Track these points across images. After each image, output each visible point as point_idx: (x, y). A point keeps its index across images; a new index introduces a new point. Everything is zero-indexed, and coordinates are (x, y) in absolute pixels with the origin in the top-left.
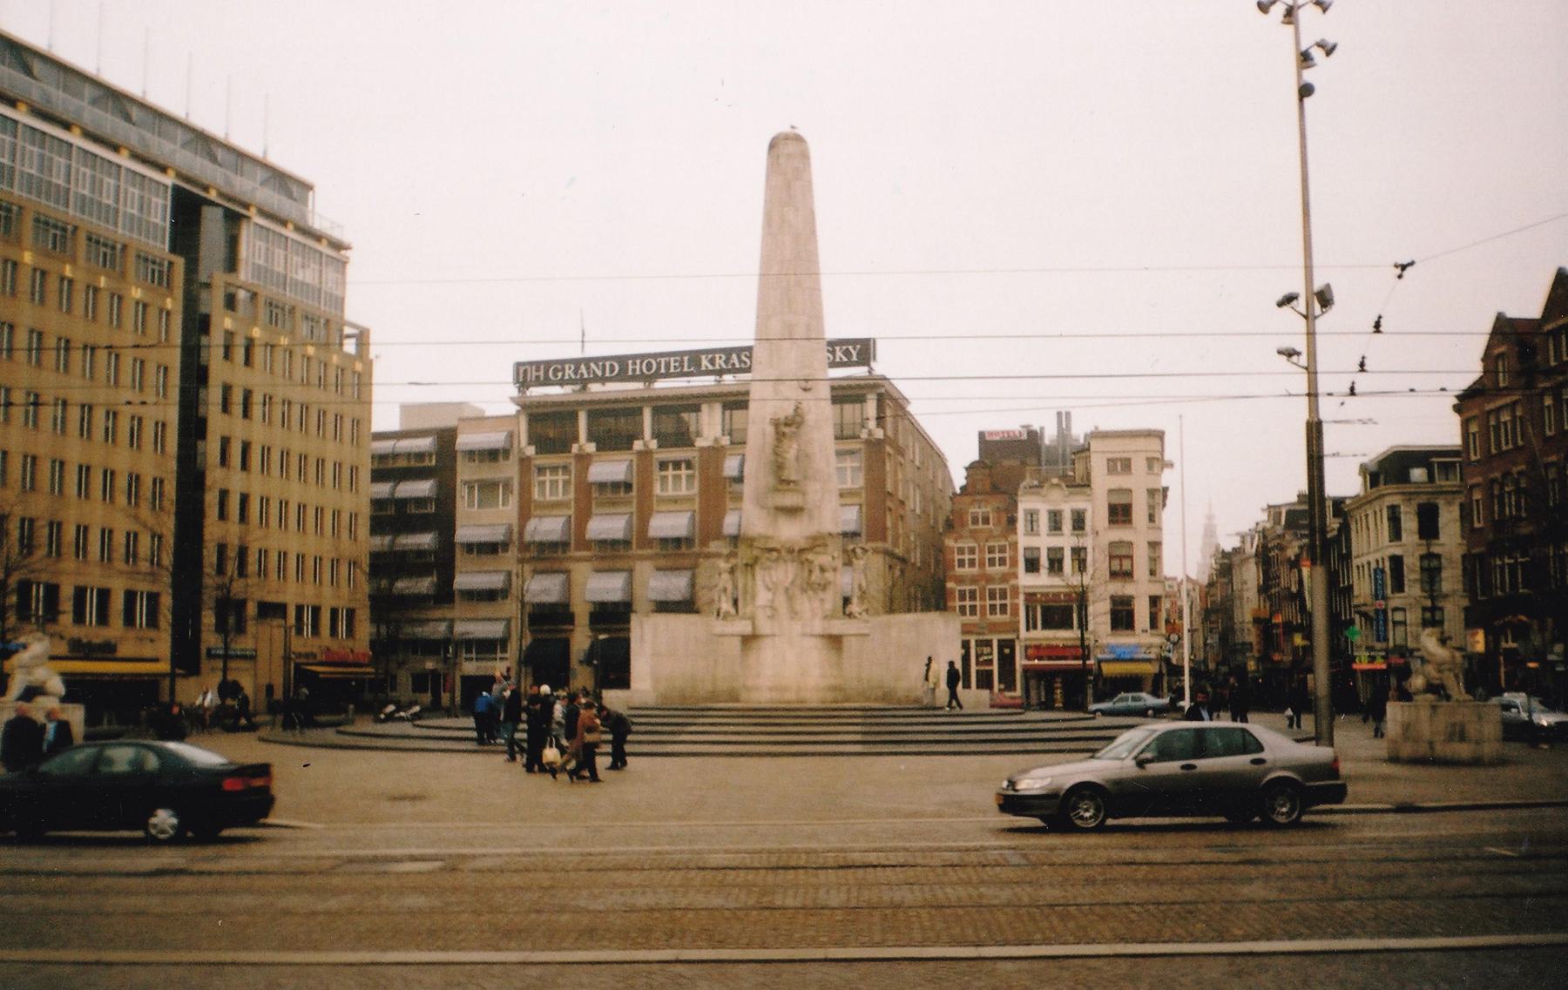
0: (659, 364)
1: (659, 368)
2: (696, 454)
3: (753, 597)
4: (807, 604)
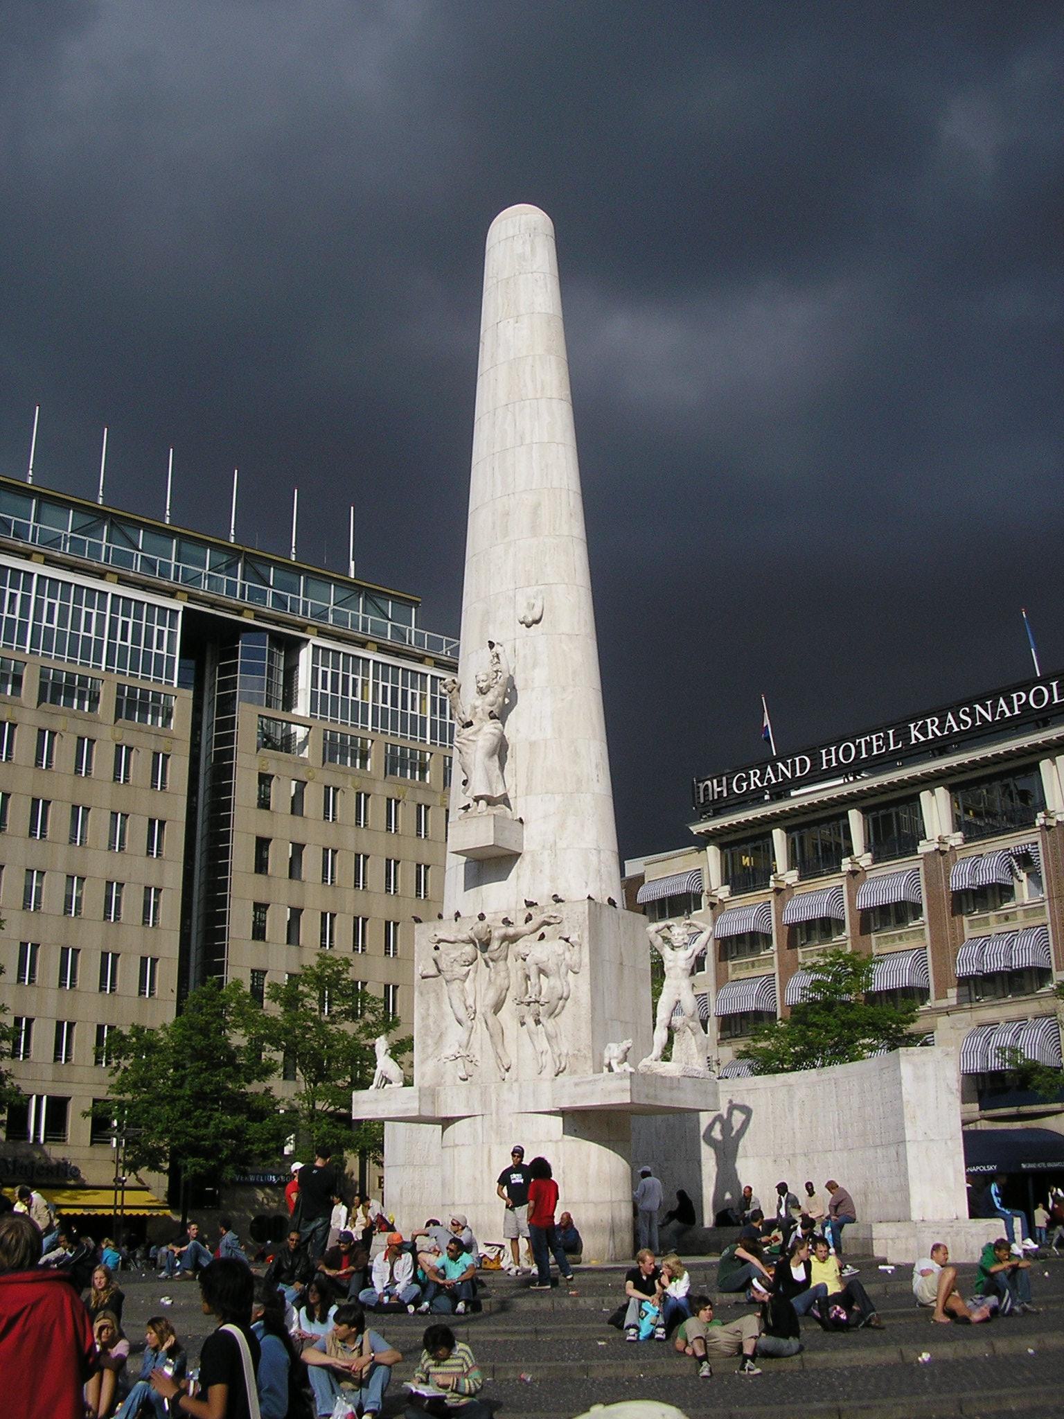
0: (858, 747)
1: (859, 752)
2: (920, 864)
3: (440, 1039)
4: (528, 1051)
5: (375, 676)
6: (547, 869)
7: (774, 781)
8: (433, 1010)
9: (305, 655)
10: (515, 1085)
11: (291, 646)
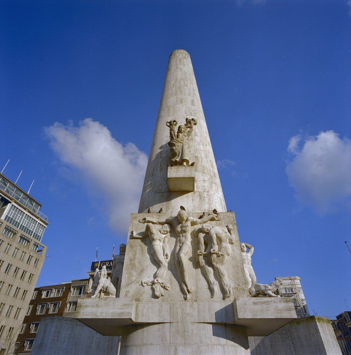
5: (25, 218)
6: (207, 199)
7: (112, 265)
8: (138, 255)
9: (9, 205)
10: (195, 304)
11: (6, 202)
